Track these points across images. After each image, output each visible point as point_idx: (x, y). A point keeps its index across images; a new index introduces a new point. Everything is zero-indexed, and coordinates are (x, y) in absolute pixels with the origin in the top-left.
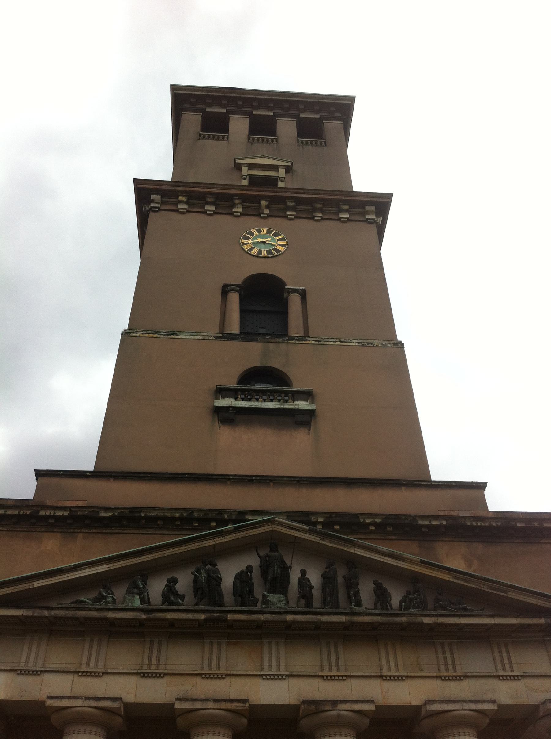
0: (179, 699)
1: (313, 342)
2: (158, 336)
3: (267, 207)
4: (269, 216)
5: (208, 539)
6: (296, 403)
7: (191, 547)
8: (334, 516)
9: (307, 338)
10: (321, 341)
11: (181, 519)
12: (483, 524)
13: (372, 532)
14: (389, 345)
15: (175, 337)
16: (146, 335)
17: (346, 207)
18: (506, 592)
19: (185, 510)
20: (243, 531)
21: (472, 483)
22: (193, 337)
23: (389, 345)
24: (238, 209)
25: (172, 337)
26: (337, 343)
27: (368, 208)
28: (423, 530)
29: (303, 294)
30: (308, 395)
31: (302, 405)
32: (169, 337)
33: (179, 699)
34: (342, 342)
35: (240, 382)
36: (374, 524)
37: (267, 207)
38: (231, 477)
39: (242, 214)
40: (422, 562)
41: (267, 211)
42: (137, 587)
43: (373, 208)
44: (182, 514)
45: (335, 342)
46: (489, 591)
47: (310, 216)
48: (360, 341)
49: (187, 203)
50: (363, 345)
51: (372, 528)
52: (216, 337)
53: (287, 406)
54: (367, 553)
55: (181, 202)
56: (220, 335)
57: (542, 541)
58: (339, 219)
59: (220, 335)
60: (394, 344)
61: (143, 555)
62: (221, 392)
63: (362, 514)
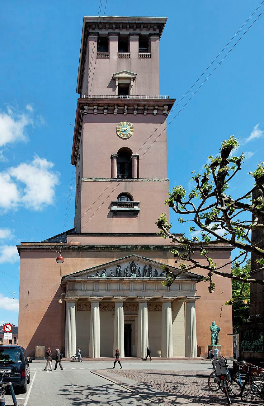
1: (141, 181)
2: (93, 181)
4: (127, 114)
6: (135, 207)
9: (139, 179)
15: (98, 181)
16: (89, 181)
22: (103, 181)
24: (116, 111)
28: (165, 249)
29: (138, 158)
30: (137, 204)
31: (136, 208)
34: (149, 180)
36: (153, 248)
42: (104, 272)
47: (142, 113)
48: (155, 179)
49: (97, 109)
52: (110, 180)
53: (132, 209)
55: (95, 109)
56: (111, 179)
58: (153, 114)
59: (111, 179)
62: (113, 204)
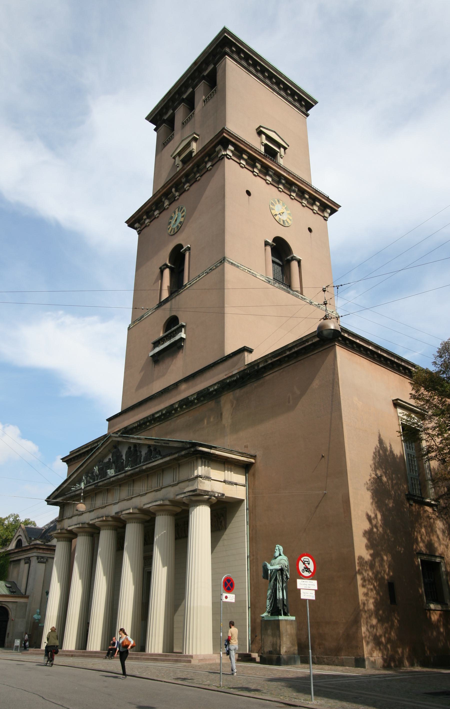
0: (91, 520)
3: (176, 191)
5: (97, 452)
7: (94, 457)
8: (180, 402)
10: (191, 283)
11: (138, 426)
12: (234, 379)
13: (197, 403)
14: (218, 265)
17: (207, 159)
18: (168, 444)
19: (137, 422)
20: (104, 444)
21: (240, 349)
23: (218, 265)
25: (142, 319)
26: (198, 279)
27: (217, 149)
32: (141, 320)
33: (91, 520)
35: (166, 331)
37: (176, 191)
38: (155, 395)
39: (170, 205)
40: (146, 438)
41: (177, 194)
43: (220, 147)
44: (144, 421)
45: (196, 279)
46: (165, 445)
50: (208, 273)
51: (214, 393)
54: (134, 440)
57: (264, 376)
60: (220, 262)
61: (83, 466)
63: (189, 396)
